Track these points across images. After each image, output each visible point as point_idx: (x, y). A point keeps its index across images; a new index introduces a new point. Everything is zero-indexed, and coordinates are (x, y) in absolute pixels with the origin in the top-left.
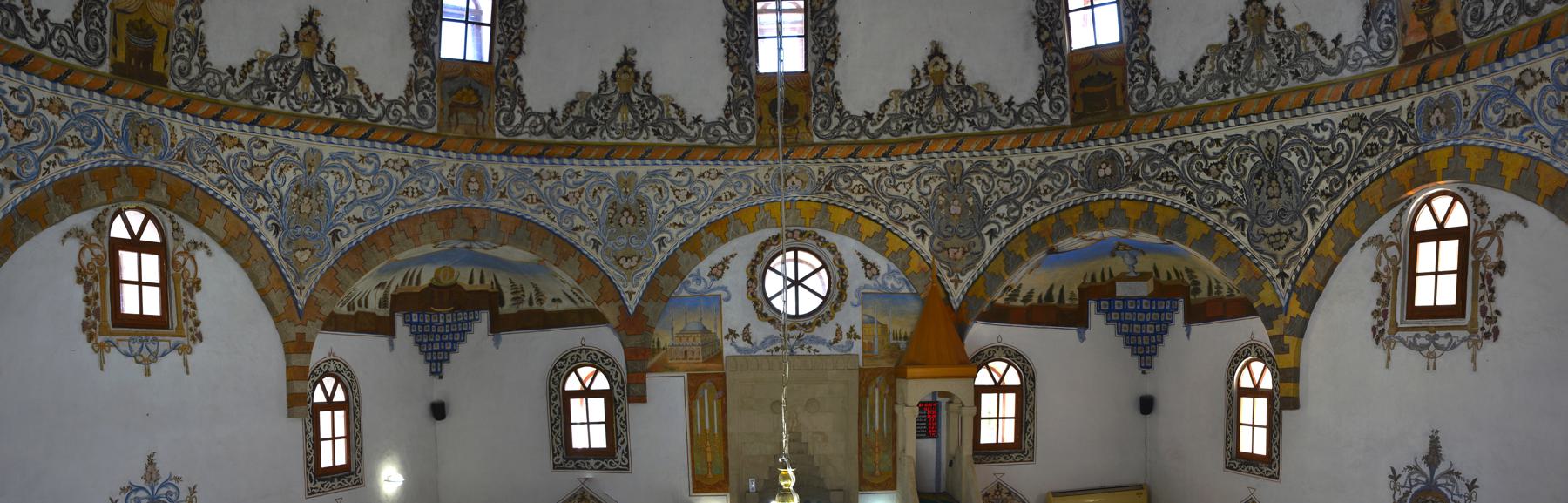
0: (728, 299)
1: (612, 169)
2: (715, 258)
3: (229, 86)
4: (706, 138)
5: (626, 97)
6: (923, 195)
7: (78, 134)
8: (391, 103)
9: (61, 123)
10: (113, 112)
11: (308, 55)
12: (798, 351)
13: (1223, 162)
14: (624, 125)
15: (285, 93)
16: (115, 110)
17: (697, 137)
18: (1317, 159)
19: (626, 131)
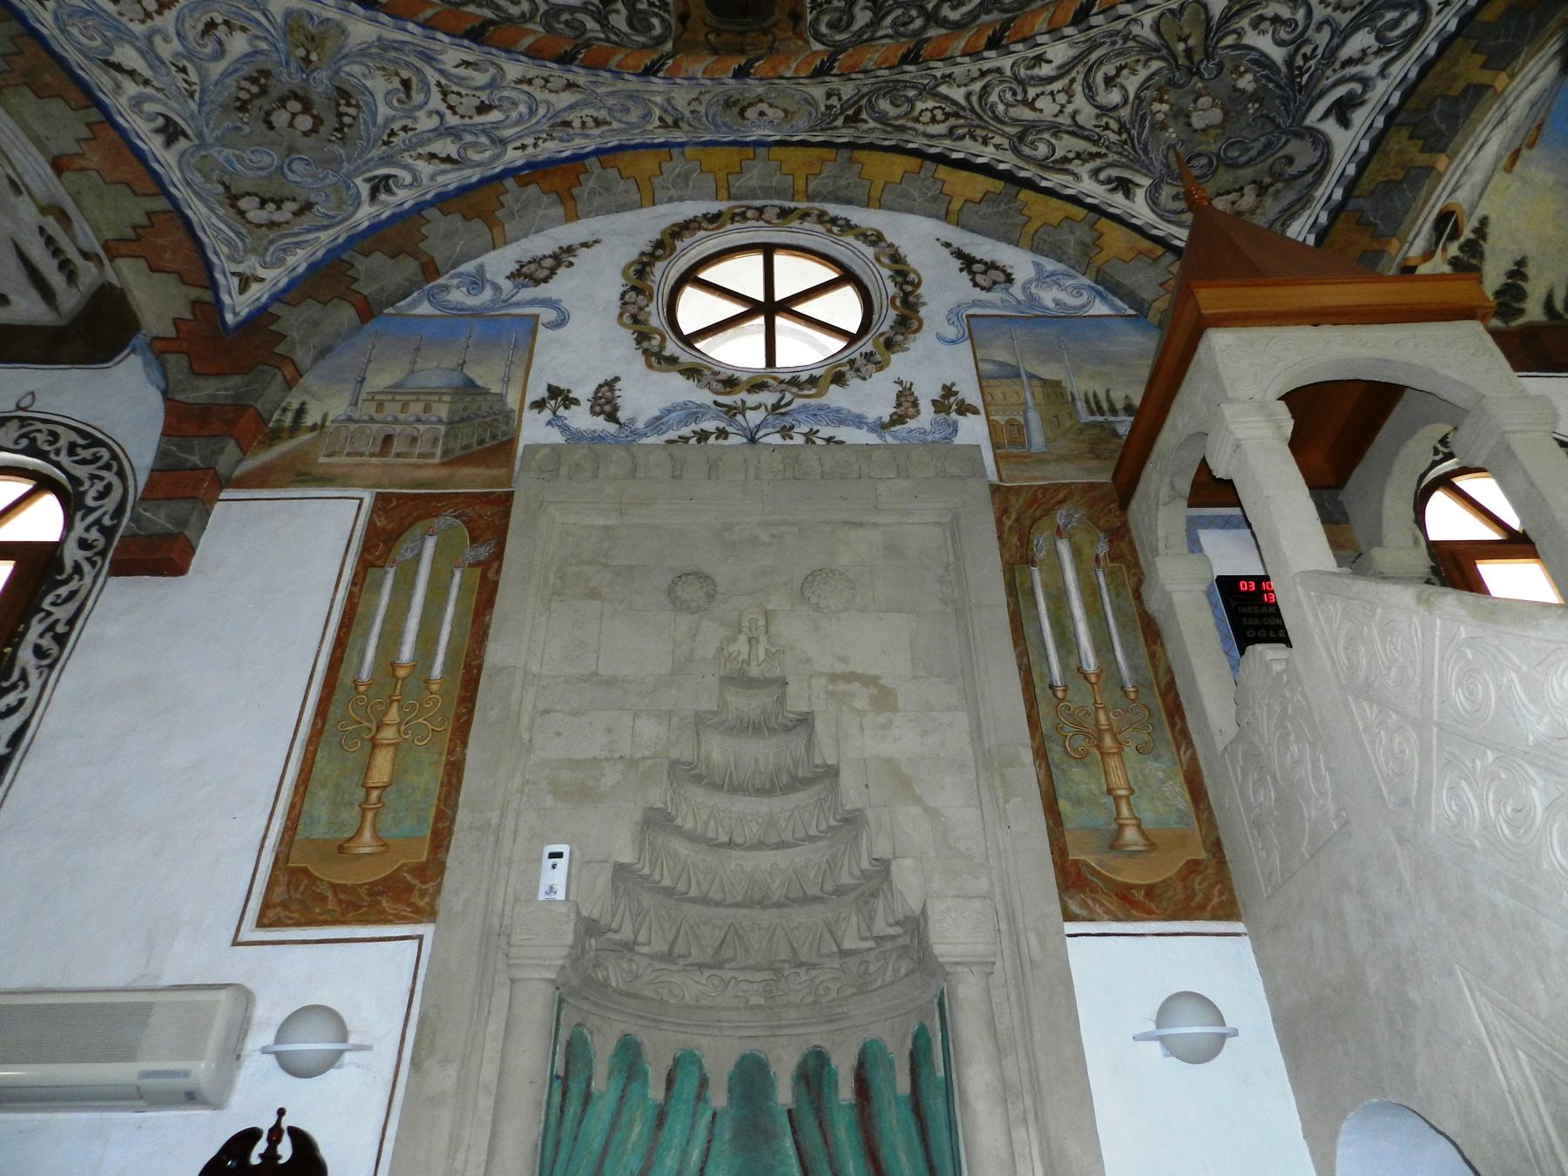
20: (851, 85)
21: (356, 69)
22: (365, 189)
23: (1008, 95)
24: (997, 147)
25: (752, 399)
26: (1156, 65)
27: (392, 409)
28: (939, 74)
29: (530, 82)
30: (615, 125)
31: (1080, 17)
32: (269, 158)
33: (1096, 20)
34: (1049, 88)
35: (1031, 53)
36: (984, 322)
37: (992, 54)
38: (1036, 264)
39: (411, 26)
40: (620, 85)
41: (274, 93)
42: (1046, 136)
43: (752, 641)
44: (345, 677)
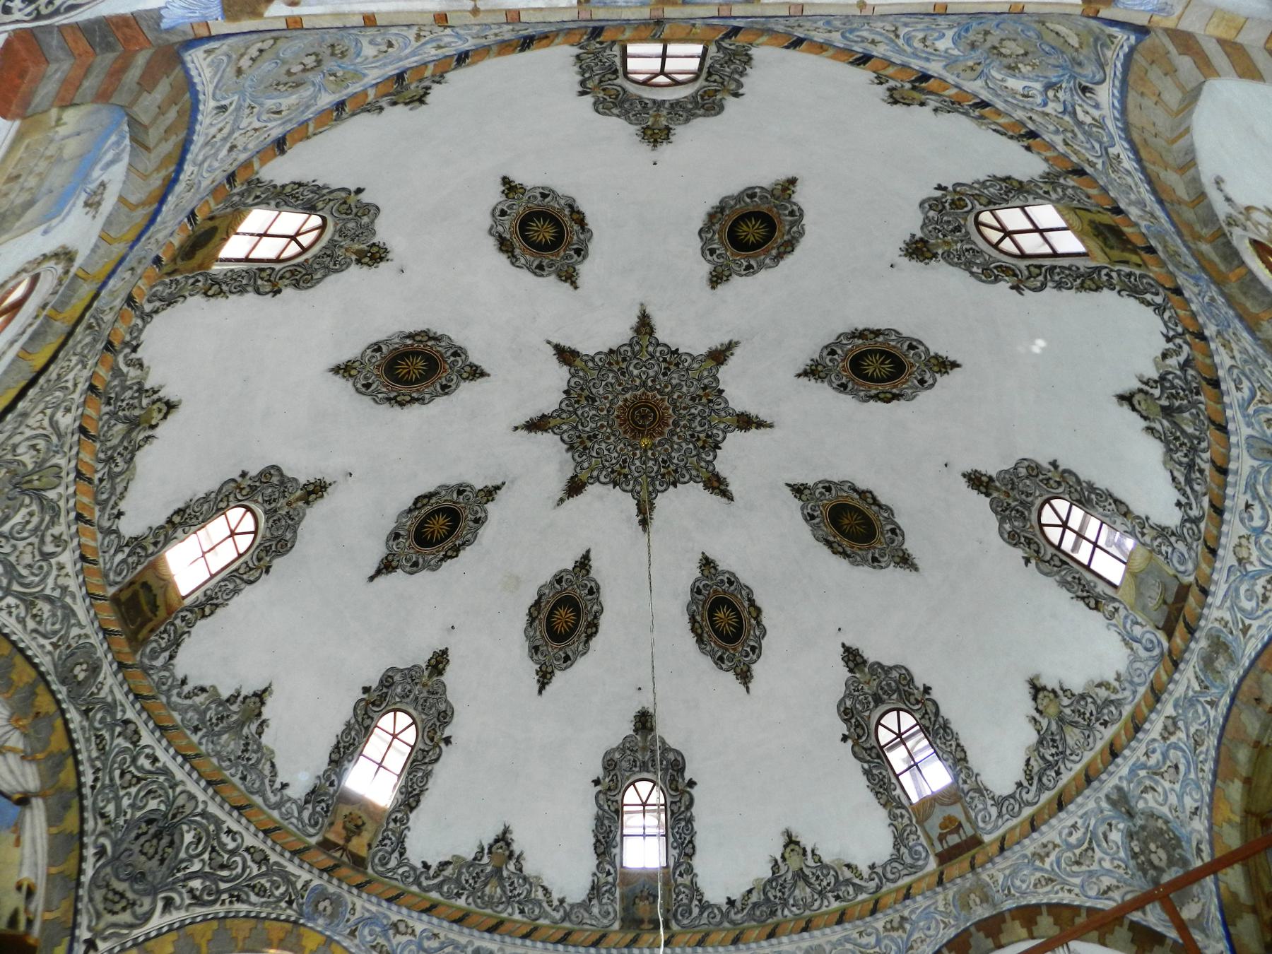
13: (139, 780)
18: (206, 856)
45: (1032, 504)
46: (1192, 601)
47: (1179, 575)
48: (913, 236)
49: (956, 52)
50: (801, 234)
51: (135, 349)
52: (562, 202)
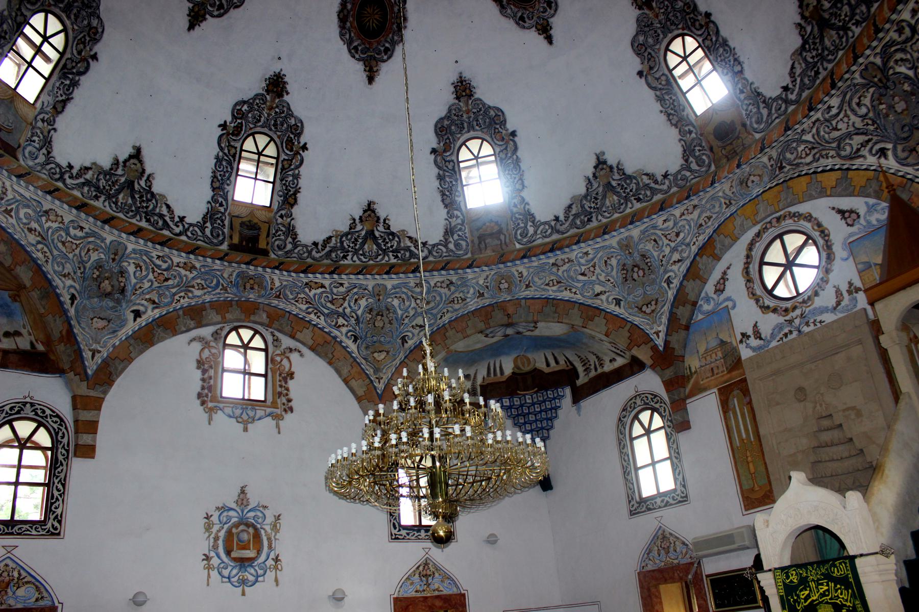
0: (734, 307)
1: (612, 240)
2: (716, 275)
3: (314, 253)
4: (677, 185)
5: (609, 187)
6: (863, 117)
7: (203, 282)
8: (434, 246)
9: (191, 276)
10: (229, 271)
11: (370, 228)
12: (806, 329)
14: (613, 206)
15: (356, 252)
16: (231, 270)
17: (670, 188)
19: (615, 209)
20: (774, 150)
21: (641, 246)
22: (665, 285)
23: (826, 129)
24: (832, 157)
25: (794, 314)
26: (872, 90)
27: (708, 358)
28: (799, 131)
29: (683, 214)
30: (714, 216)
31: (833, 86)
32: (640, 291)
33: (840, 84)
34: (839, 118)
35: (826, 107)
36: (855, 243)
37: (812, 113)
38: (866, 203)
39: (645, 220)
40: (708, 195)
41: (630, 270)
42: (847, 141)
43: (821, 405)
44: (735, 447)
45: (69, 17)
46: (14, 165)
47: (21, 149)
48: (288, 93)
49: (389, 300)
50: (342, 35)
51: (786, 89)
52: (509, 11)
